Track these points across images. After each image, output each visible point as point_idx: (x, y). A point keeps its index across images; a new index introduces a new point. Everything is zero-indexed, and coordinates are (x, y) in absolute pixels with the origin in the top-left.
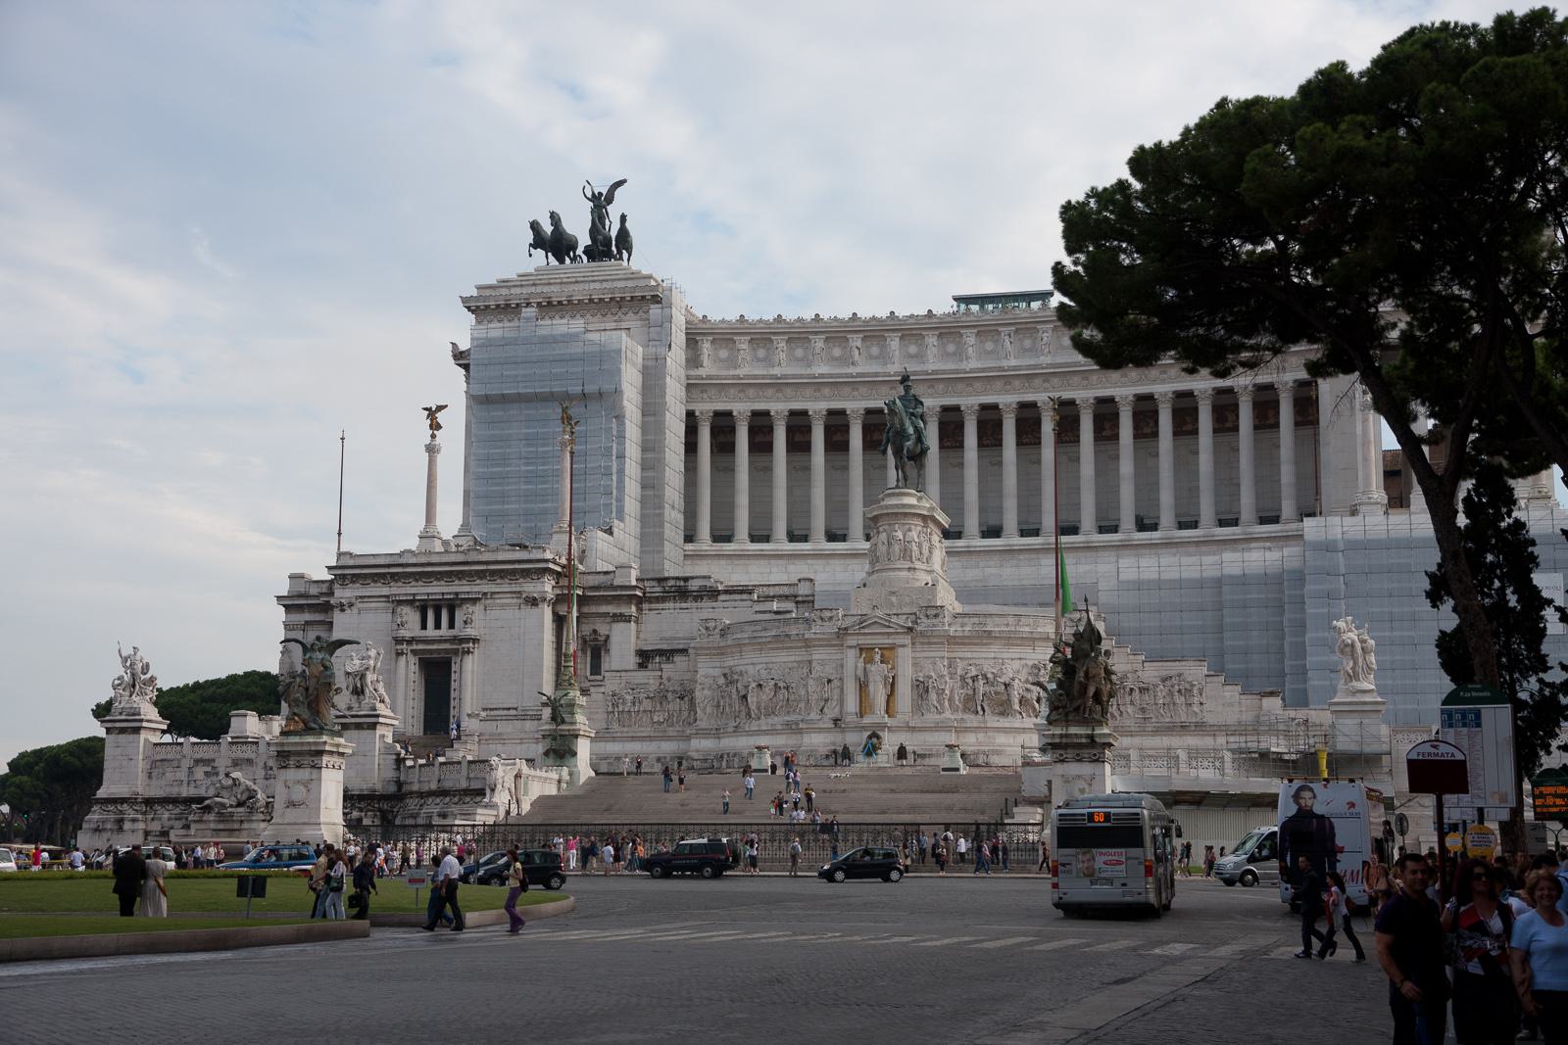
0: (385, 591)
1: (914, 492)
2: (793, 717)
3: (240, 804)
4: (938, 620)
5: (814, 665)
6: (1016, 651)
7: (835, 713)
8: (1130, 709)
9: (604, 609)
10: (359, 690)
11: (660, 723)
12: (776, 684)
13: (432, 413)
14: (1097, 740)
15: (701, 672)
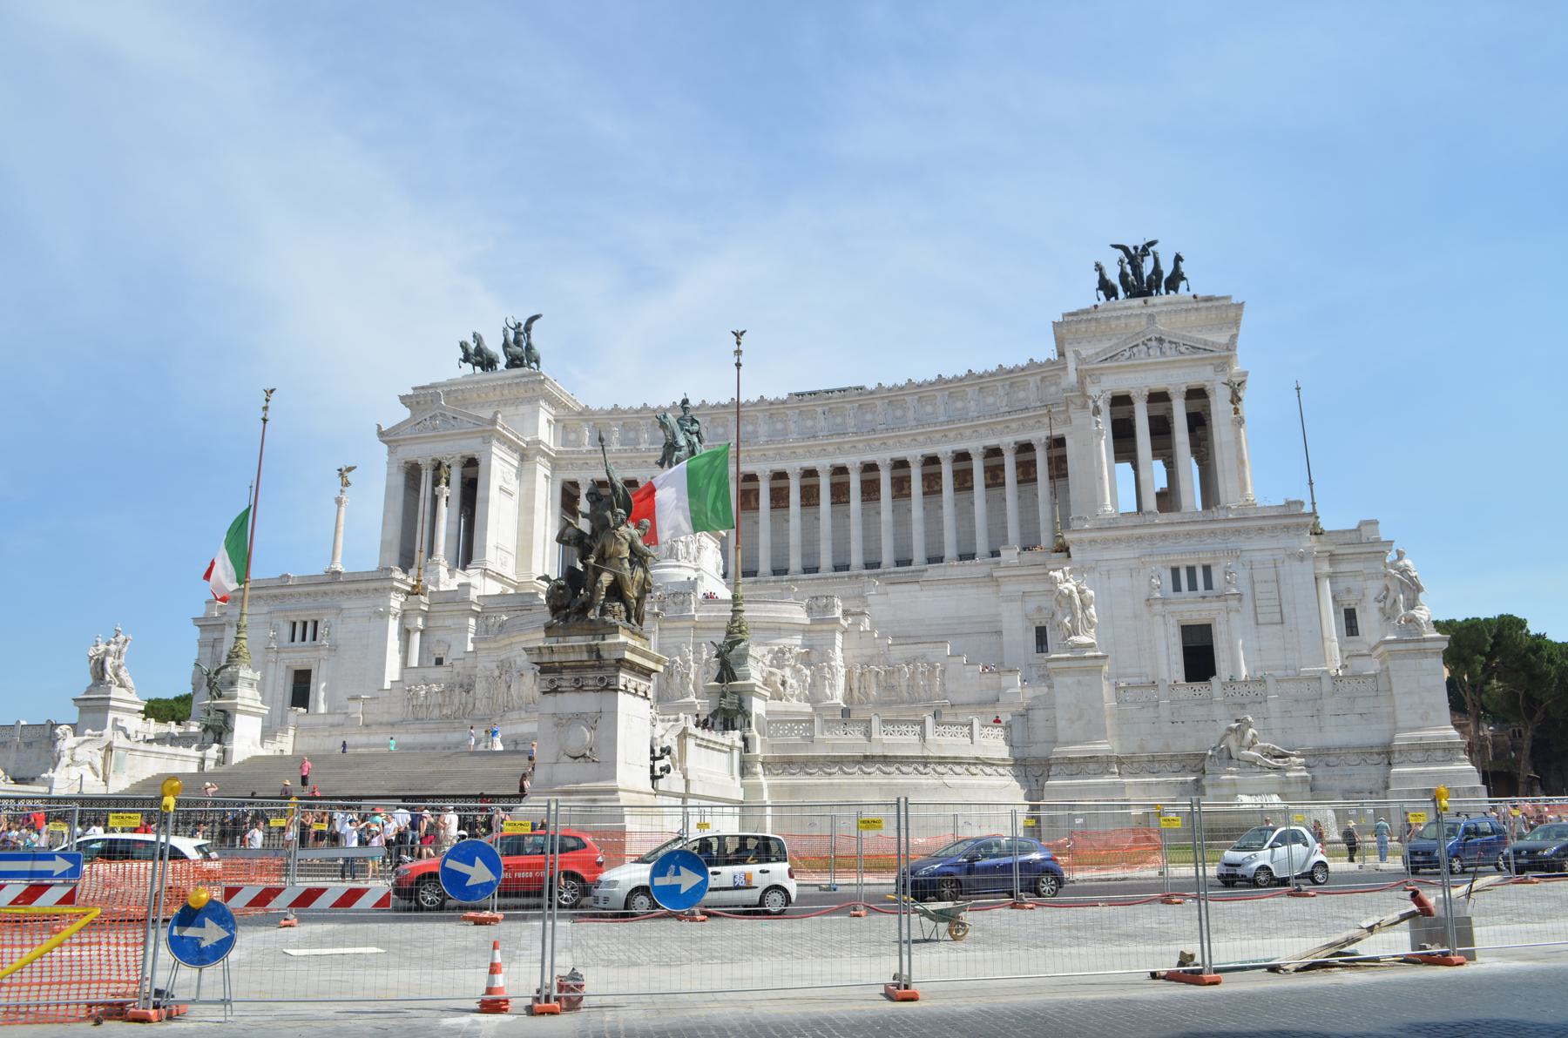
0: (265, 609)
8: (874, 692)
9: (448, 622)
14: (605, 655)
15: (480, 666)
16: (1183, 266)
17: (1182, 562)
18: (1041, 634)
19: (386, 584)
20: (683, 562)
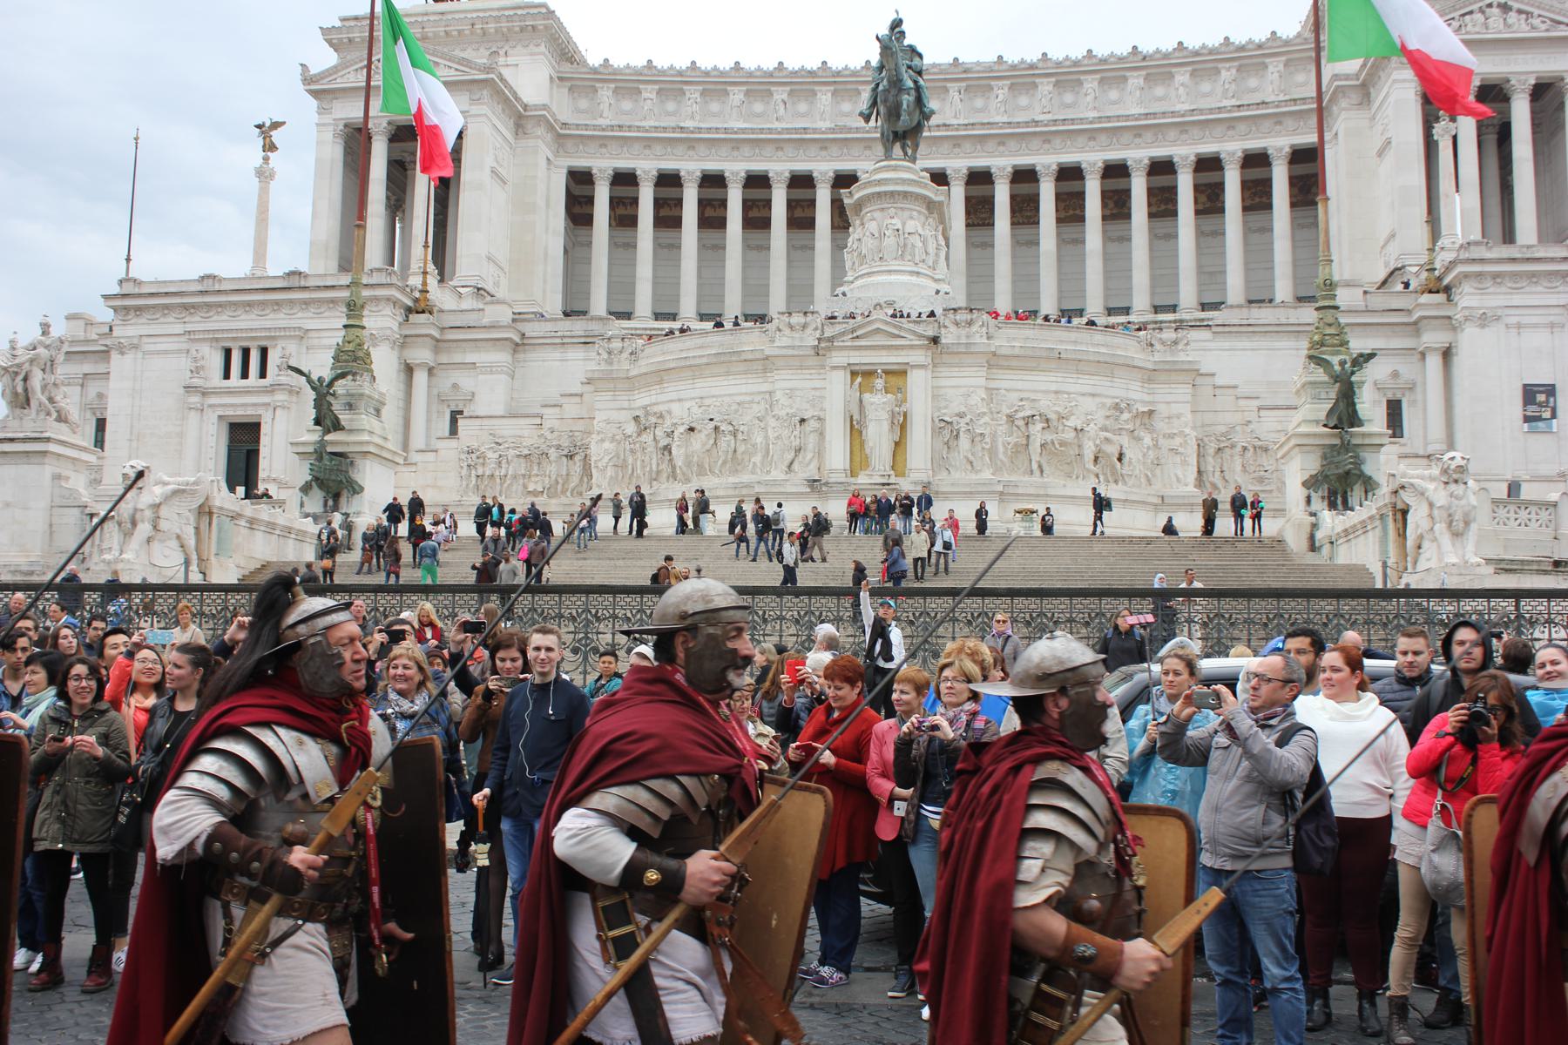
0: (179, 329)
2: (745, 478)
4: (975, 328)
5: (779, 395)
6: (1086, 383)
9: (470, 358)
10: (22, 398)
12: (716, 428)
13: (266, 130)
15: (600, 416)
18: (1394, 412)
20: (923, 269)
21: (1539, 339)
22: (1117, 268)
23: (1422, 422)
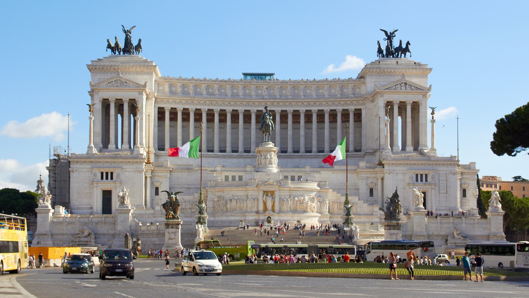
0: (88, 166)
1: (271, 143)
3: (86, 237)
7: (256, 210)
9: (160, 174)
11: (193, 212)
15: (209, 197)
16: (410, 47)
17: (419, 172)
18: (371, 190)
19: (142, 160)
21: (400, 177)
22: (308, 138)
23: (377, 193)
